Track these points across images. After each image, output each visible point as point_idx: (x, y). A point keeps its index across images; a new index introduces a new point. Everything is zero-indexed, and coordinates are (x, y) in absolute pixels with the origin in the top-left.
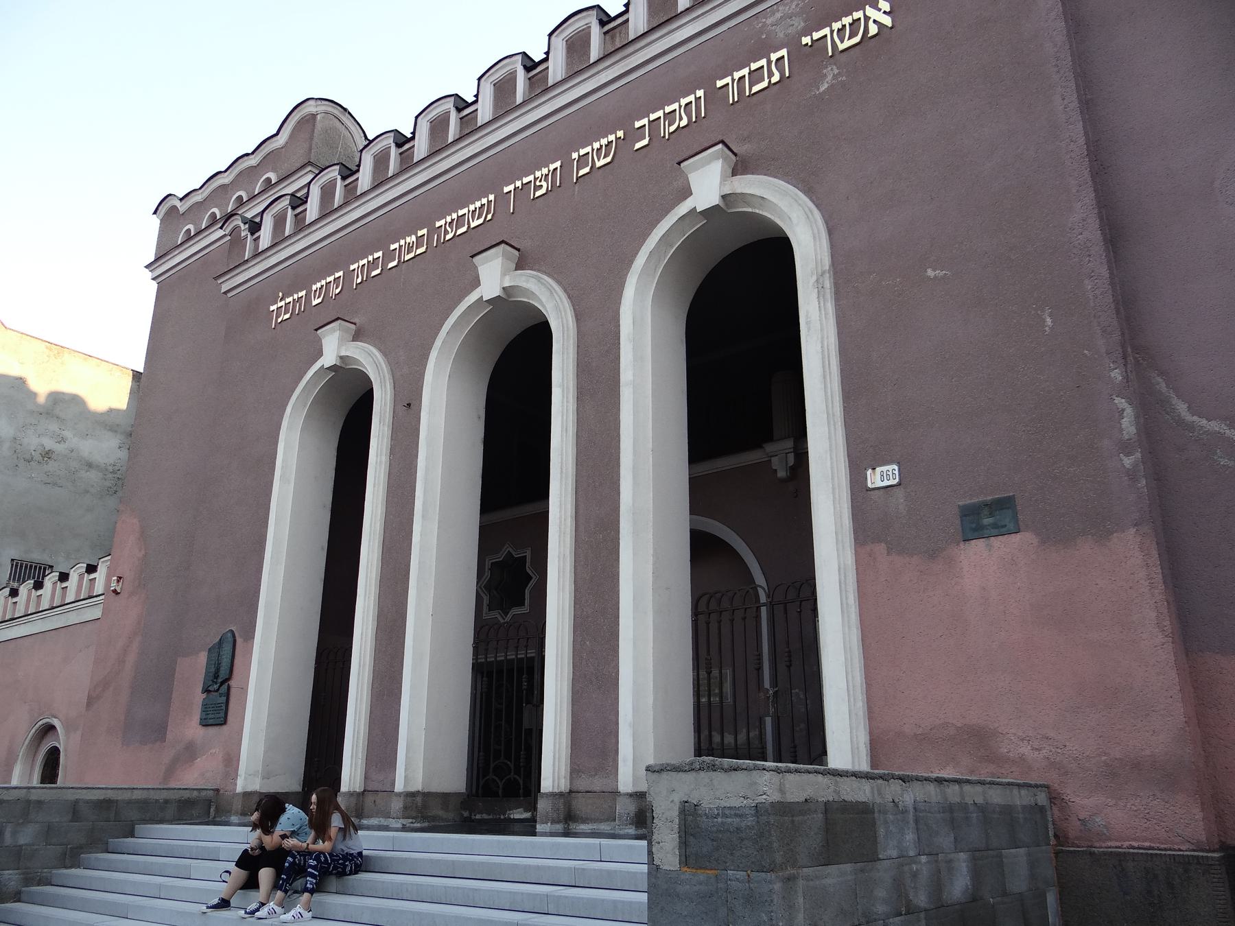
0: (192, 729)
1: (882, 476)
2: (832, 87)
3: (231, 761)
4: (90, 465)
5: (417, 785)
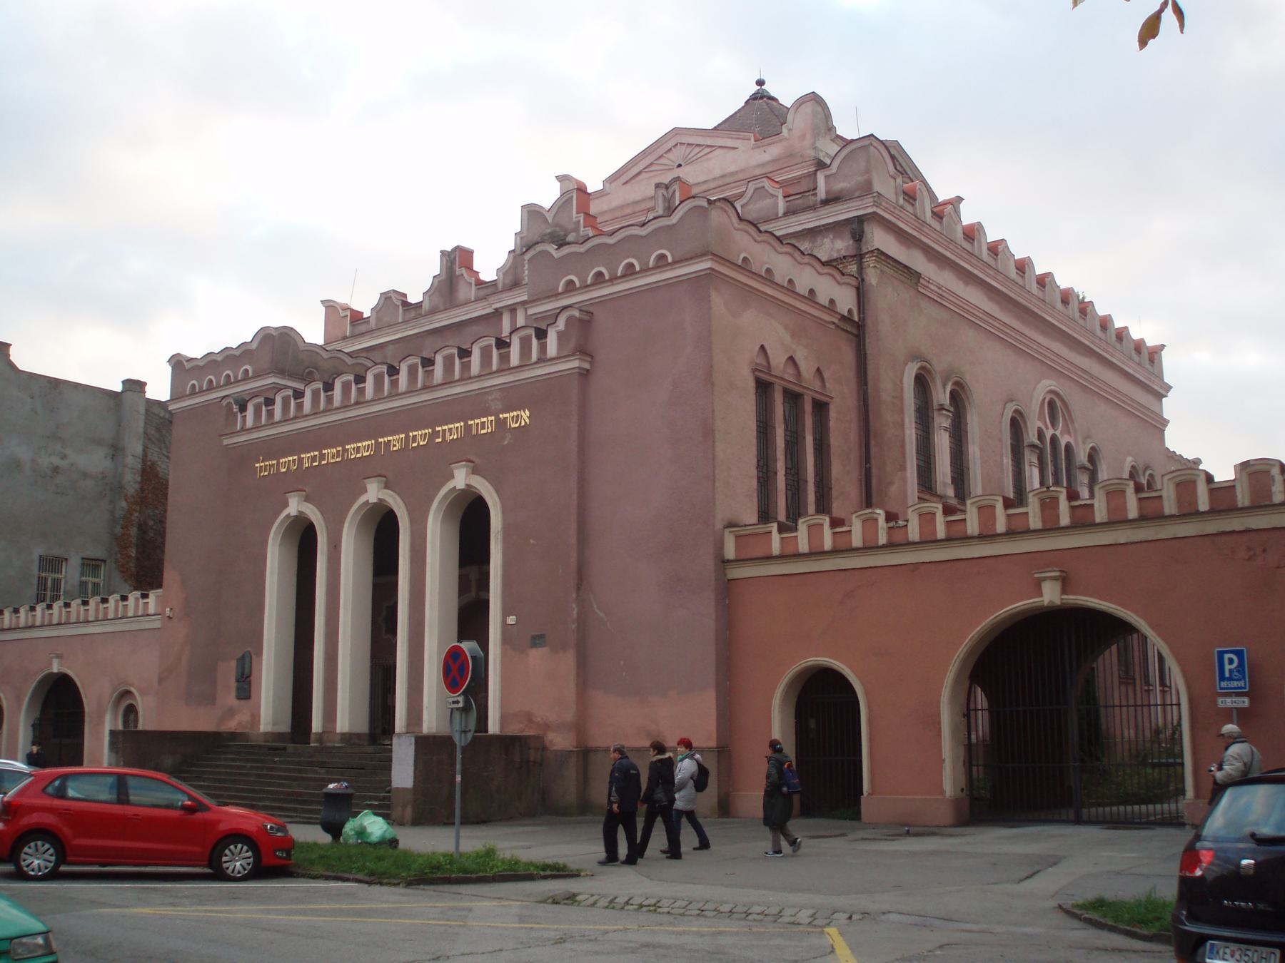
0: (230, 699)
1: (511, 620)
3: (255, 717)
4: (85, 475)
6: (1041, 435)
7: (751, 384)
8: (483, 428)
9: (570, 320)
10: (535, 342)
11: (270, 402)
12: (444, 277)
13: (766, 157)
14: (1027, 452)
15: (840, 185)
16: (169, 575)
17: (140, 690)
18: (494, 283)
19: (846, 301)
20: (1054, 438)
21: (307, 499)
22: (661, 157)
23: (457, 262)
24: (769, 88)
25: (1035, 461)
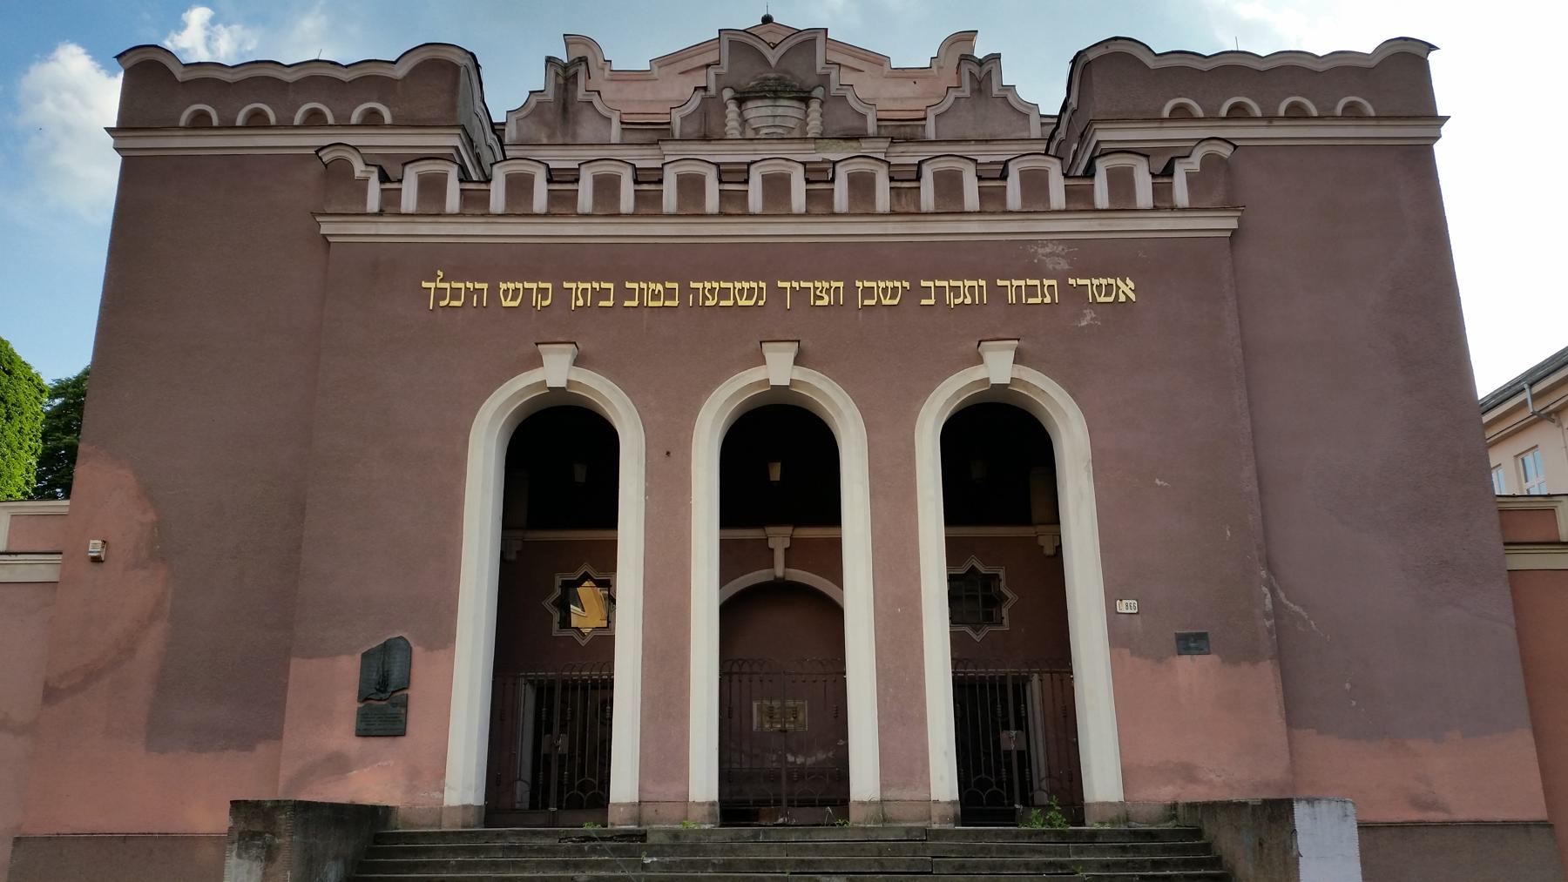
0: (341, 735)
1: (1126, 606)
2: (1089, 326)
9: (1208, 160)
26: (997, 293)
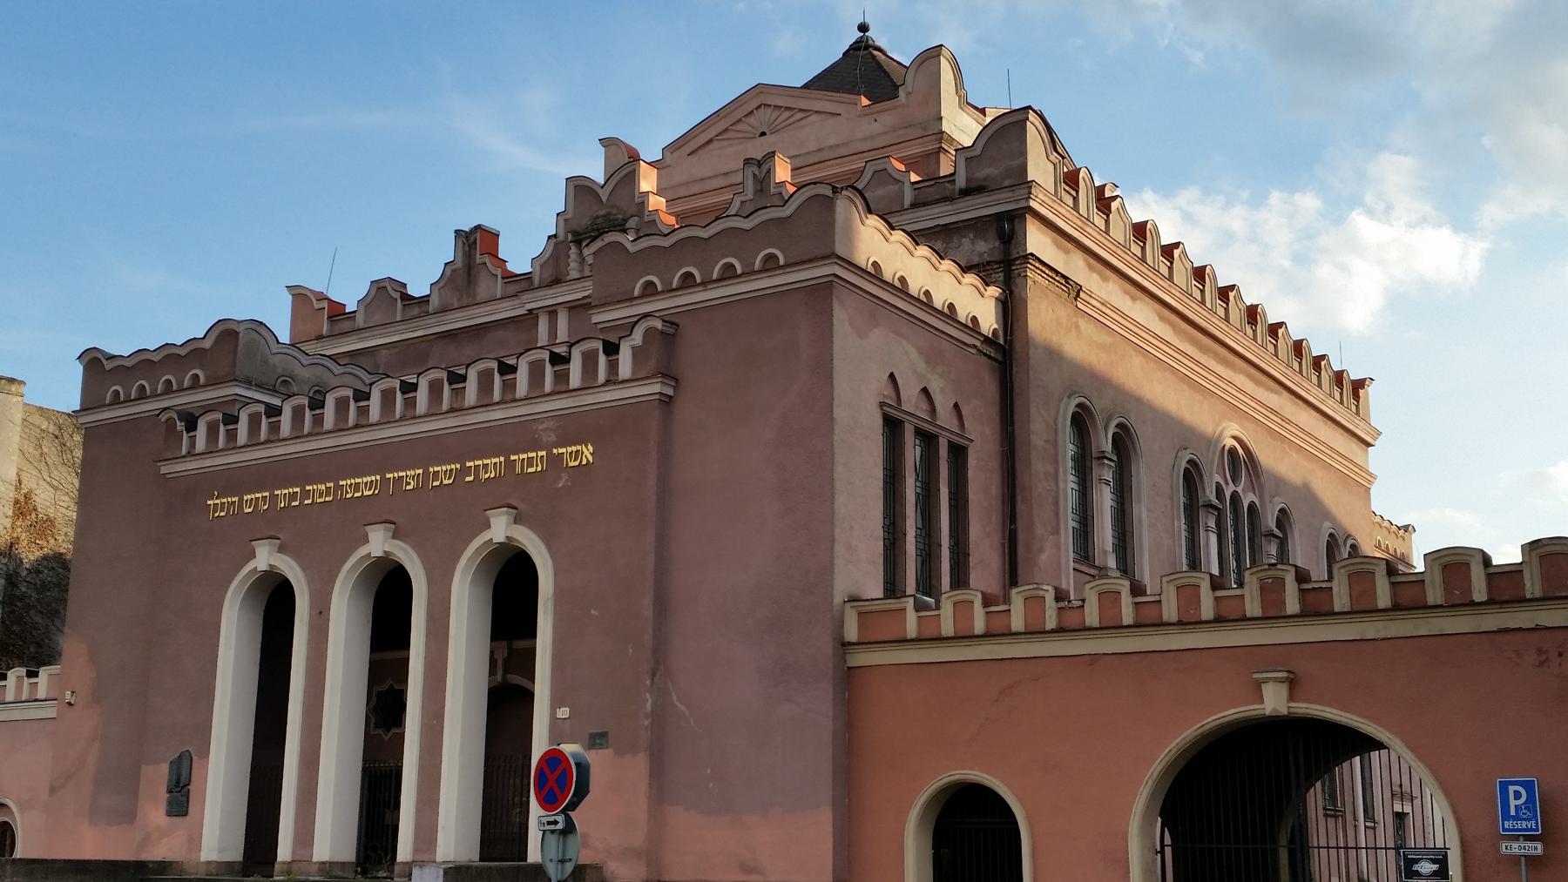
1: (563, 713)
3: (195, 841)
5: (326, 858)
6: (1220, 492)
7: (879, 421)
8: (530, 465)
9: (649, 332)
10: (602, 359)
11: (231, 420)
12: (459, 264)
13: (876, 128)
14: (1202, 512)
15: (986, 172)
16: (71, 645)
17: (24, 807)
18: (527, 277)
19: (989, 321)
20: (1235, 496)
21: (281, 549)
22: (739, 121)
23: (477, 245)
24: (877, 36)
25: (1212, 523)
26: (510, 465)
